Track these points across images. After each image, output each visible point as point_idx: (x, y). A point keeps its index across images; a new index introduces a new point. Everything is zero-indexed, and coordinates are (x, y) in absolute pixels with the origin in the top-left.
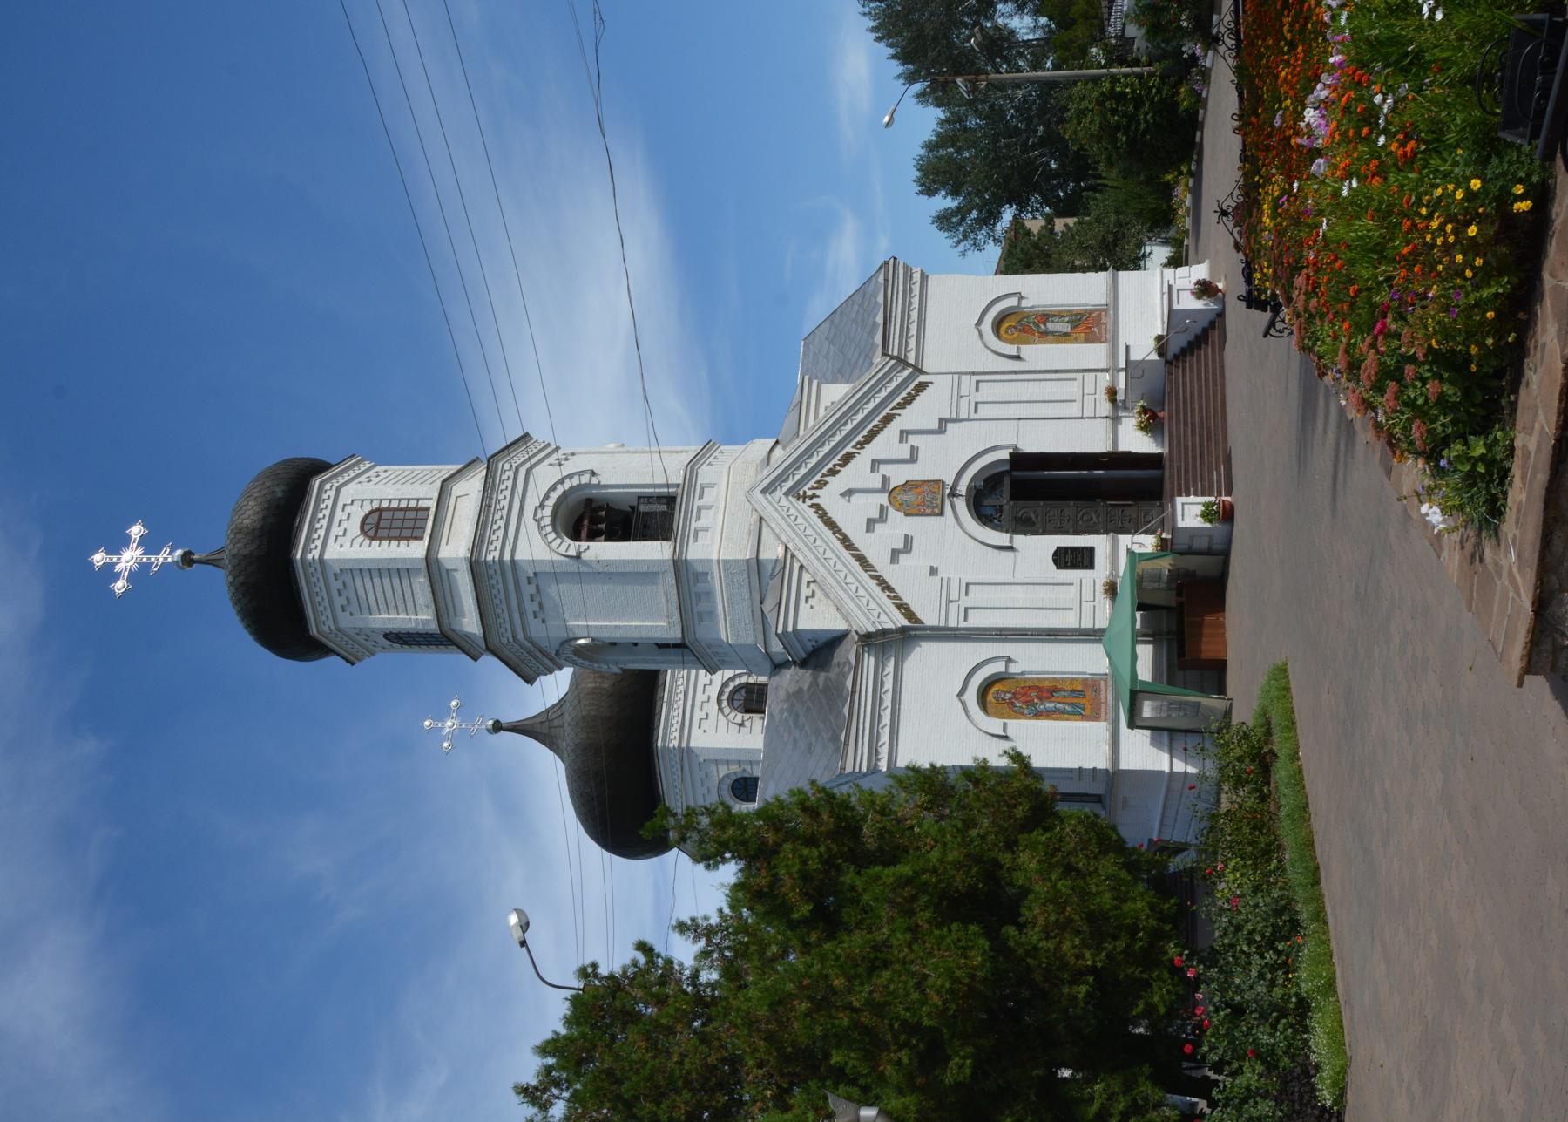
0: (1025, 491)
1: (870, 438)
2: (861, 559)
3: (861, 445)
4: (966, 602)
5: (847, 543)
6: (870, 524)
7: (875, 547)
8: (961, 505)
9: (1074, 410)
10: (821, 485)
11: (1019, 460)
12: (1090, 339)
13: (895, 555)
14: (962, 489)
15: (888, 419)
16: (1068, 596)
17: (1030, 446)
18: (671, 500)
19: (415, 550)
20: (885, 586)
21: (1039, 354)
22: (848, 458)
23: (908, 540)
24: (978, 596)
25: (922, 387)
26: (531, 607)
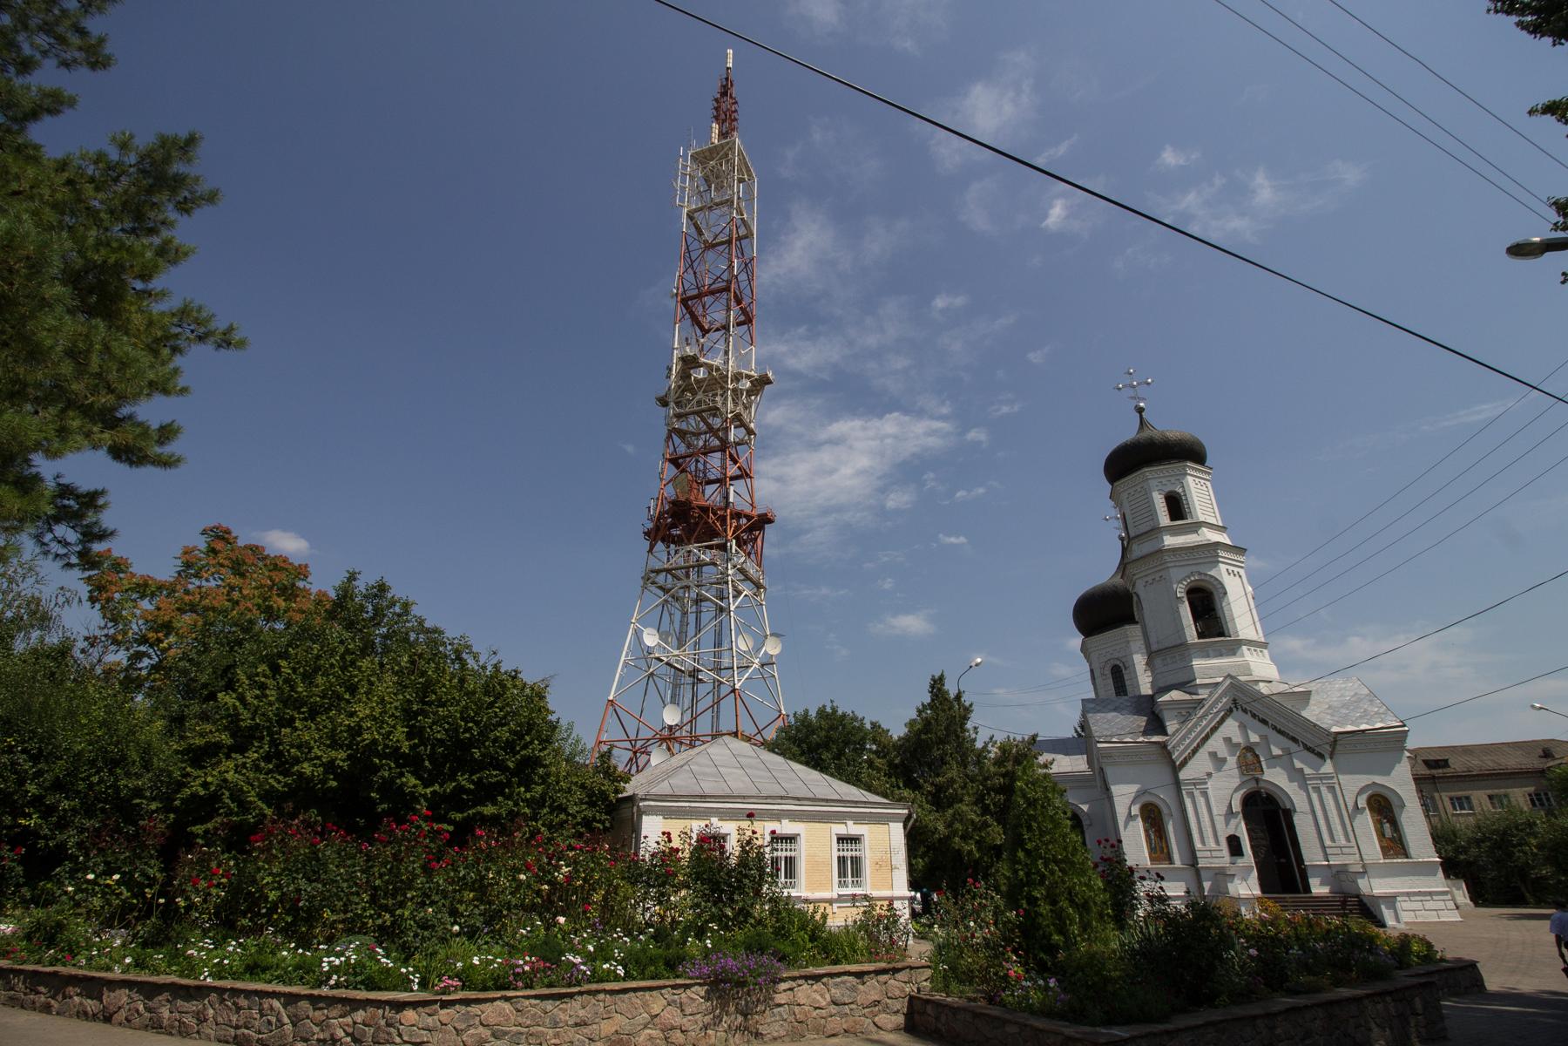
0: (1268, 818)
1: (1280, 732)
2: (1207, 738)
3: (1275, 728)
4: (1197, 793)
5: (1214, 729)
6: (1228, 740)
7: (1216, 744)
8: (1252, 785)
9: (1328, 842)
10: (1245, 711)
11: (1289, 814)
12: (1386, 851)
13: (1213, 755)
14: (1262, 784)
15: (1294, 740)
16: (1212, 844)
17: (1297, 819)
18: (1222, 634)
19: (1164, 519)
20: (1195, 751)
21: (1366, 823)
22: (1264, 722)
23: (1224, 760)
24: (1201, 801)
25: (1321, 756)
26: (1149, 579)
